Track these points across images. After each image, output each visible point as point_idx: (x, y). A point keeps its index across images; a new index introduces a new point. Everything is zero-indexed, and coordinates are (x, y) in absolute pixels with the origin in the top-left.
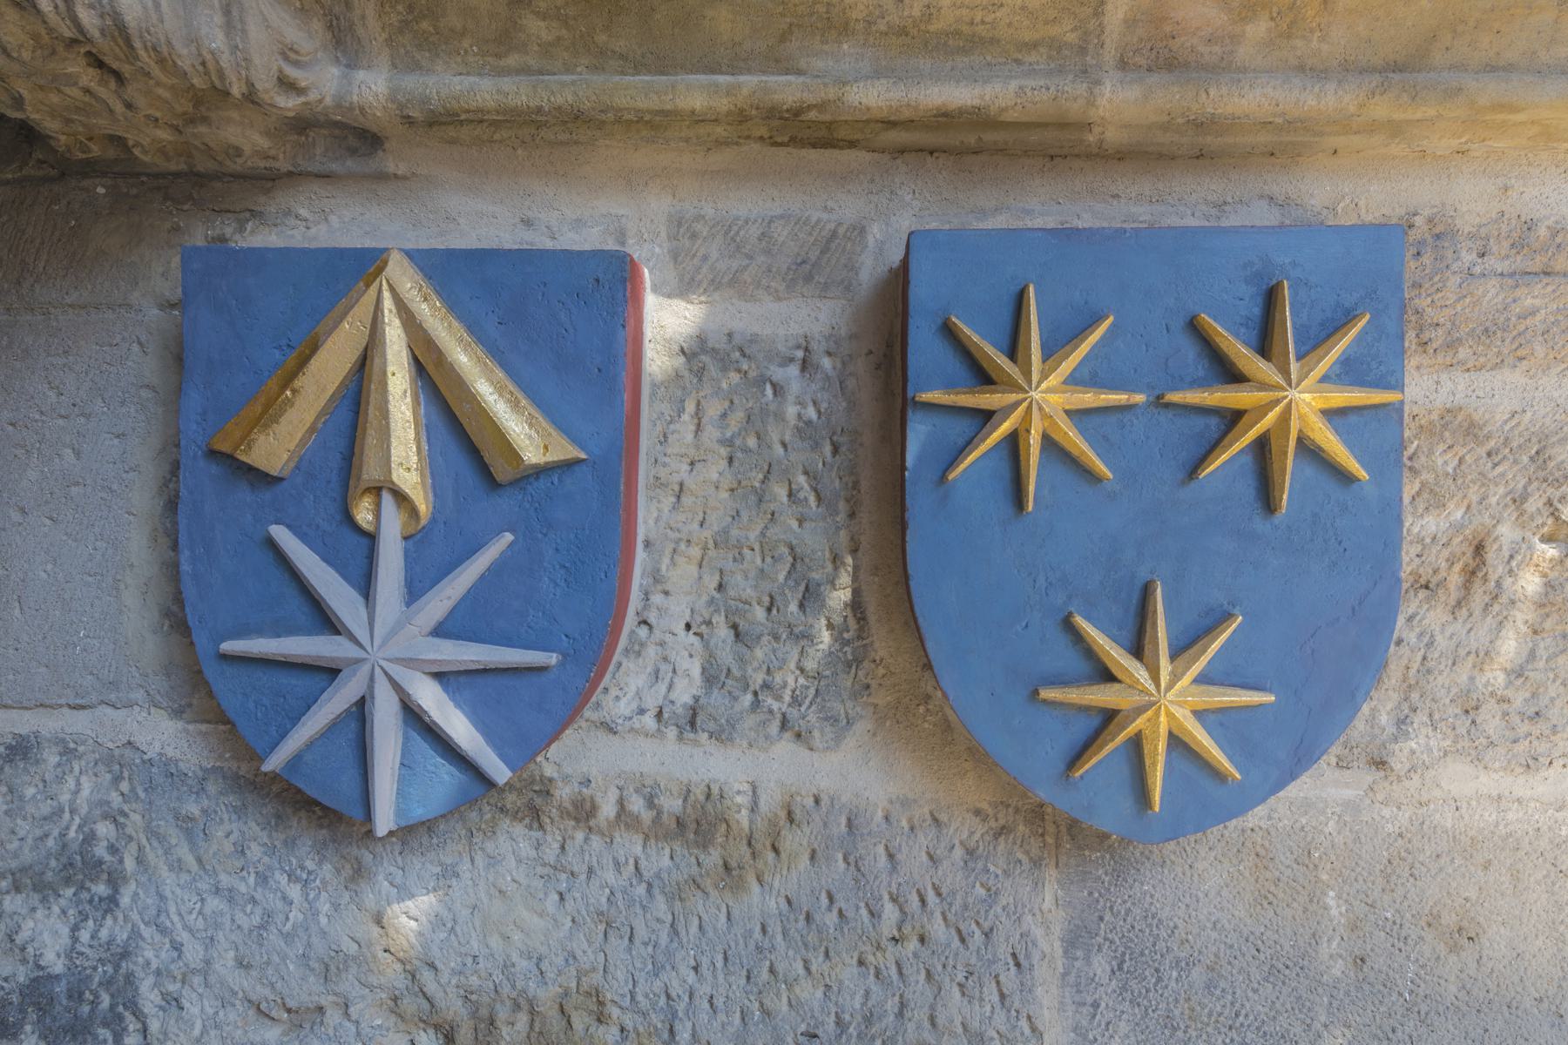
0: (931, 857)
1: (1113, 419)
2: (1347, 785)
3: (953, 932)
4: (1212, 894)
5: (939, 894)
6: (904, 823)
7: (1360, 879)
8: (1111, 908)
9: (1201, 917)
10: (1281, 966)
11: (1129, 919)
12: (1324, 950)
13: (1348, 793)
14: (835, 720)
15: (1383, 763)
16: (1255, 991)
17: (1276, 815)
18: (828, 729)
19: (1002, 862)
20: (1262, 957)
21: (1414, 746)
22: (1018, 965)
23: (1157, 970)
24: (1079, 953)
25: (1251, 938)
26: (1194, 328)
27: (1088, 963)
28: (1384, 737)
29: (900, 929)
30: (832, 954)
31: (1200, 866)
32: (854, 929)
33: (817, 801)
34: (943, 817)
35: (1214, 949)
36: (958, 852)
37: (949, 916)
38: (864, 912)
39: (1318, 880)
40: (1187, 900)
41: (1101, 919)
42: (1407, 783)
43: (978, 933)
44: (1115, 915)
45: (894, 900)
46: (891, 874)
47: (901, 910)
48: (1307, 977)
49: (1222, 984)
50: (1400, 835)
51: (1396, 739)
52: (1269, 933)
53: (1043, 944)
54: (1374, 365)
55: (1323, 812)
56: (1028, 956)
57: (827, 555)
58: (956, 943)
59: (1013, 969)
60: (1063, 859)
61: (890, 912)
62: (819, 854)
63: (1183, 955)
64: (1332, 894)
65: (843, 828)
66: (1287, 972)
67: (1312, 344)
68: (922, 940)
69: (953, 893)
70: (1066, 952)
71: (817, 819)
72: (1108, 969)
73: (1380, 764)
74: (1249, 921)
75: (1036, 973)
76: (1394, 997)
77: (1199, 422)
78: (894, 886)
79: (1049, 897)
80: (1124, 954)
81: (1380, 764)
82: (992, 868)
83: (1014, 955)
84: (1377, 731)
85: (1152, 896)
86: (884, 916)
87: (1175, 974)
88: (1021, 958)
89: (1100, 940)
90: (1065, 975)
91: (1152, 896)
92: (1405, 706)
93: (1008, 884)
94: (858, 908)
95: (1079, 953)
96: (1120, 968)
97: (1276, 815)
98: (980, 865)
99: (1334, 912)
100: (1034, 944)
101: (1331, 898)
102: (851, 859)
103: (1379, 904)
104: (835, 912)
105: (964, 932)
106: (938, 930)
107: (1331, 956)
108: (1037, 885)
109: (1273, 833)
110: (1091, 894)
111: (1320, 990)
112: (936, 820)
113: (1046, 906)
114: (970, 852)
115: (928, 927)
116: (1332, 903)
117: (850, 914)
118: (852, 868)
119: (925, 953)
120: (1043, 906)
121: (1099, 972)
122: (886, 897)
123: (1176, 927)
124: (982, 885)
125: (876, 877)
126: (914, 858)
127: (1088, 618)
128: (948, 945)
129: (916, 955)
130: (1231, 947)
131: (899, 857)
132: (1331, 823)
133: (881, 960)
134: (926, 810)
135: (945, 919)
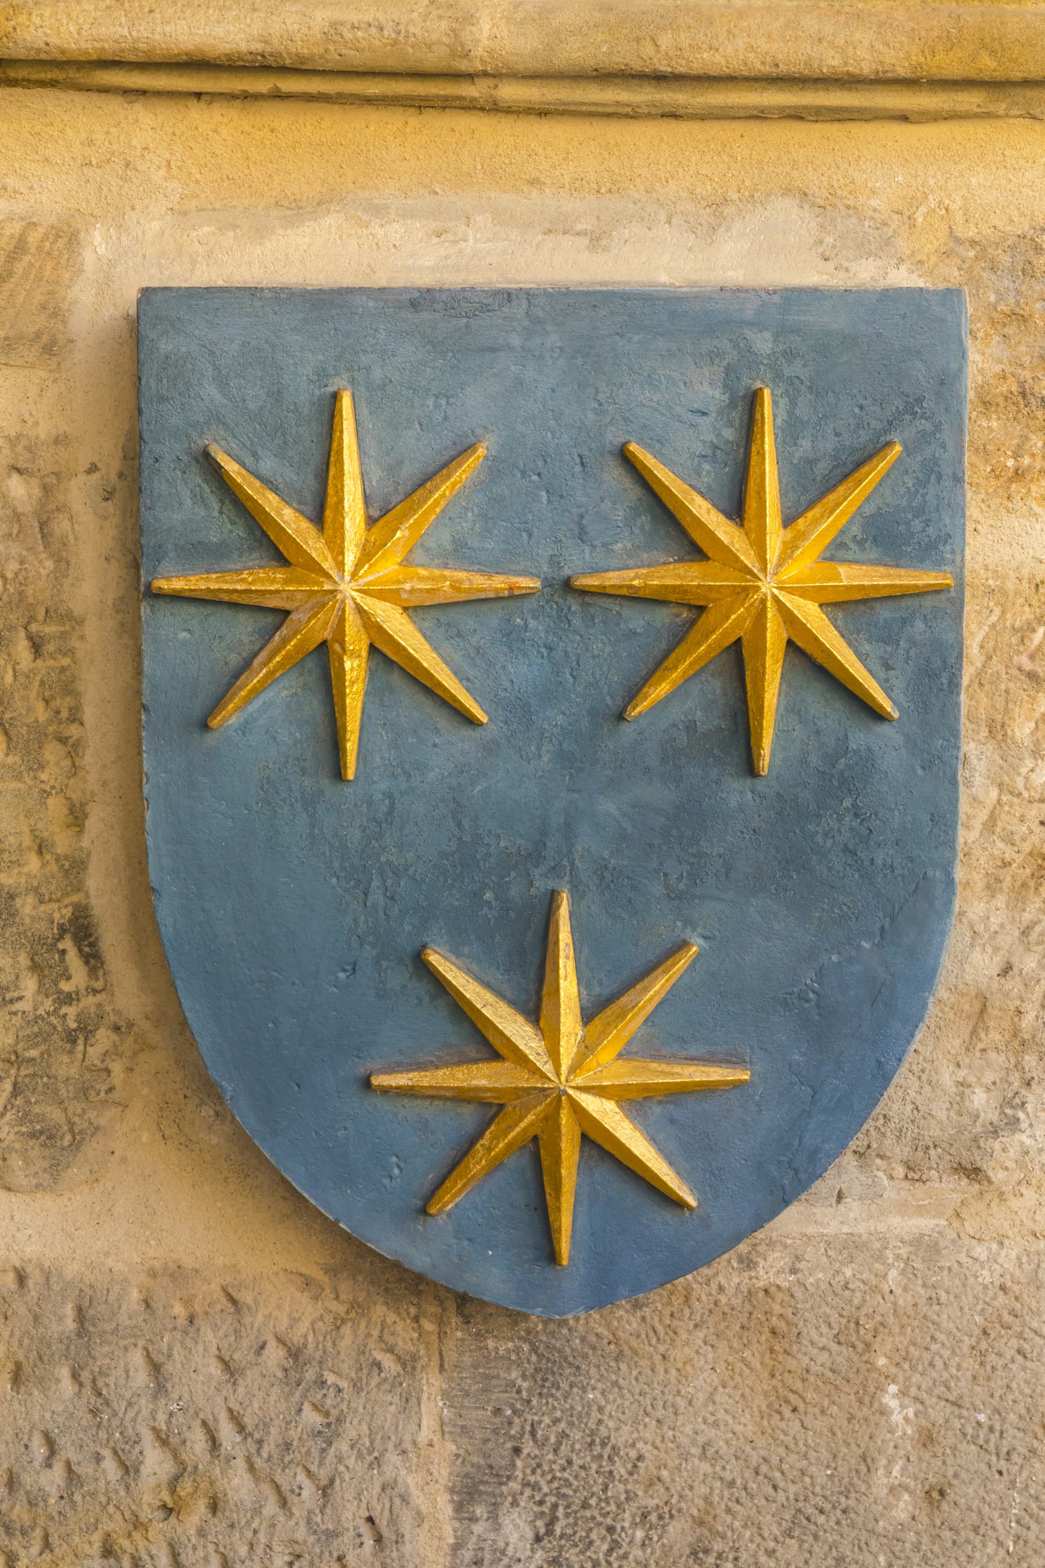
0: (226, 1365)
1: (494, 617)
2: (921, 1211)
3: (266, 1488)
4: (698, 1403)
5: (241, 1428)
6: (179, 1309)
7: (939, 1363)
8: (533, 1433)
9: (684, 1440)
10: (810, 1511)
11: (564, 1449)
12: (881, 1481)
13: (923, 1224)
14: (46, 1136)
15: (977, 1170)
16: (770, 1553)
17: (802, 1265)
18: (36, 1153)
19: (346, 1366)
20: (781, 1496)
21: (1028, 1142)
22: (379, 1539)
23: (611, 1529)
24: (480, 1511)
25: (764, 1469)
26: (626, 459)
27: (497, 1527)
28: (979, 1128)
29: (173, 1491)
30: (54, 1540)
31: (678, 1354)
32: (93, 1494)
33: (21, 1278)
34: (246, 1297)
35: (704, 1490)
36: (274, 1355)
37: (259, 1463)
38: (110, 1465)
39: (871, 1367)
40: (660, 1413)
41: (517, 1451)
42: (1014, 1203)
43: (309, 1491)
44: (541, 1444)
45: (163, 1441)
46: (155, 1397)
47: (175, 1456)
48: (852, 1525)
49: (717, 1546)
50: (1003, 1288)
51: (995, 1132)
52: (792, 1458)
53: (419, 1499)
54: (917, 525)
55: (880, 1257)
56: (393, 1520)
57: (27, 840)
58: (271, 1507)
59: (369, 1543)
60: (451, 1357)
61: (155, 1463)
62: (27, 1369)
63: (652, 1503)
64: (893, 1388)
65: (70, 1324)
66: (821, 1519)
67: (807, 493)
68: (214, 1507)
69: (265, 1425)
70: (459, 1507)
71: (22, 1310)
72: (530, 1535)
73: (973, 1173)
74: (761, 1442)
75: (407, 1548)
76: (991, 1549)
77: (636, 619)
78: (162, 1417)
79: (429, 1423)
80: (555, 1507)
81: (973, 1173)
82: (331, 1378)
83: (370, 1520)
84: (966, 1120)
85: (601, 1409)
86: (145, 1470)
87: (639, 1534)
88: (382, 1523)
89: (514, 1486)
90: (456, 1548)
91: (601, 1409)
92: (1016, 1079)
93: (359, 1403)
94: (98, 1459)
95: (480, 1511)
96: (550, 1532)
97: (802, 1265)
98: (310, 1375)
99: (897, 1418)
100: (405, 1499)
101: (890, 1397)
102: (85, 1376)
103: (966, 1402)
104: (59, 1468)
105: (285, 1488)
106: (238, 1485)
107: (892, 1489)
108: (410, 1401)
109: (799, 1294)
110: (498, 1411)
111: (873, 1543)
112: (234, 1301)
113: (424, 1436)
114: (295, 1354)
115: (221, 1484)
116: (893, 1404)
117: (85, 1470)
118: (88, 1391)
119: (217, 1526)
120: (420, 1434)
121: (513, 1539)
122: (147, 1436)
123: (640, 1458)
124: (315, 1407)
125: (130, 1404)
126: (197, 1375)
127: (456, 951)
128: (257, 1511)
129: (201, 1533)
130: (732, 1484)
131: (169, 1367)
132: (893, 1274)
133: (141, 1544)
134: (215, 1287)
135: (251, 1468)
